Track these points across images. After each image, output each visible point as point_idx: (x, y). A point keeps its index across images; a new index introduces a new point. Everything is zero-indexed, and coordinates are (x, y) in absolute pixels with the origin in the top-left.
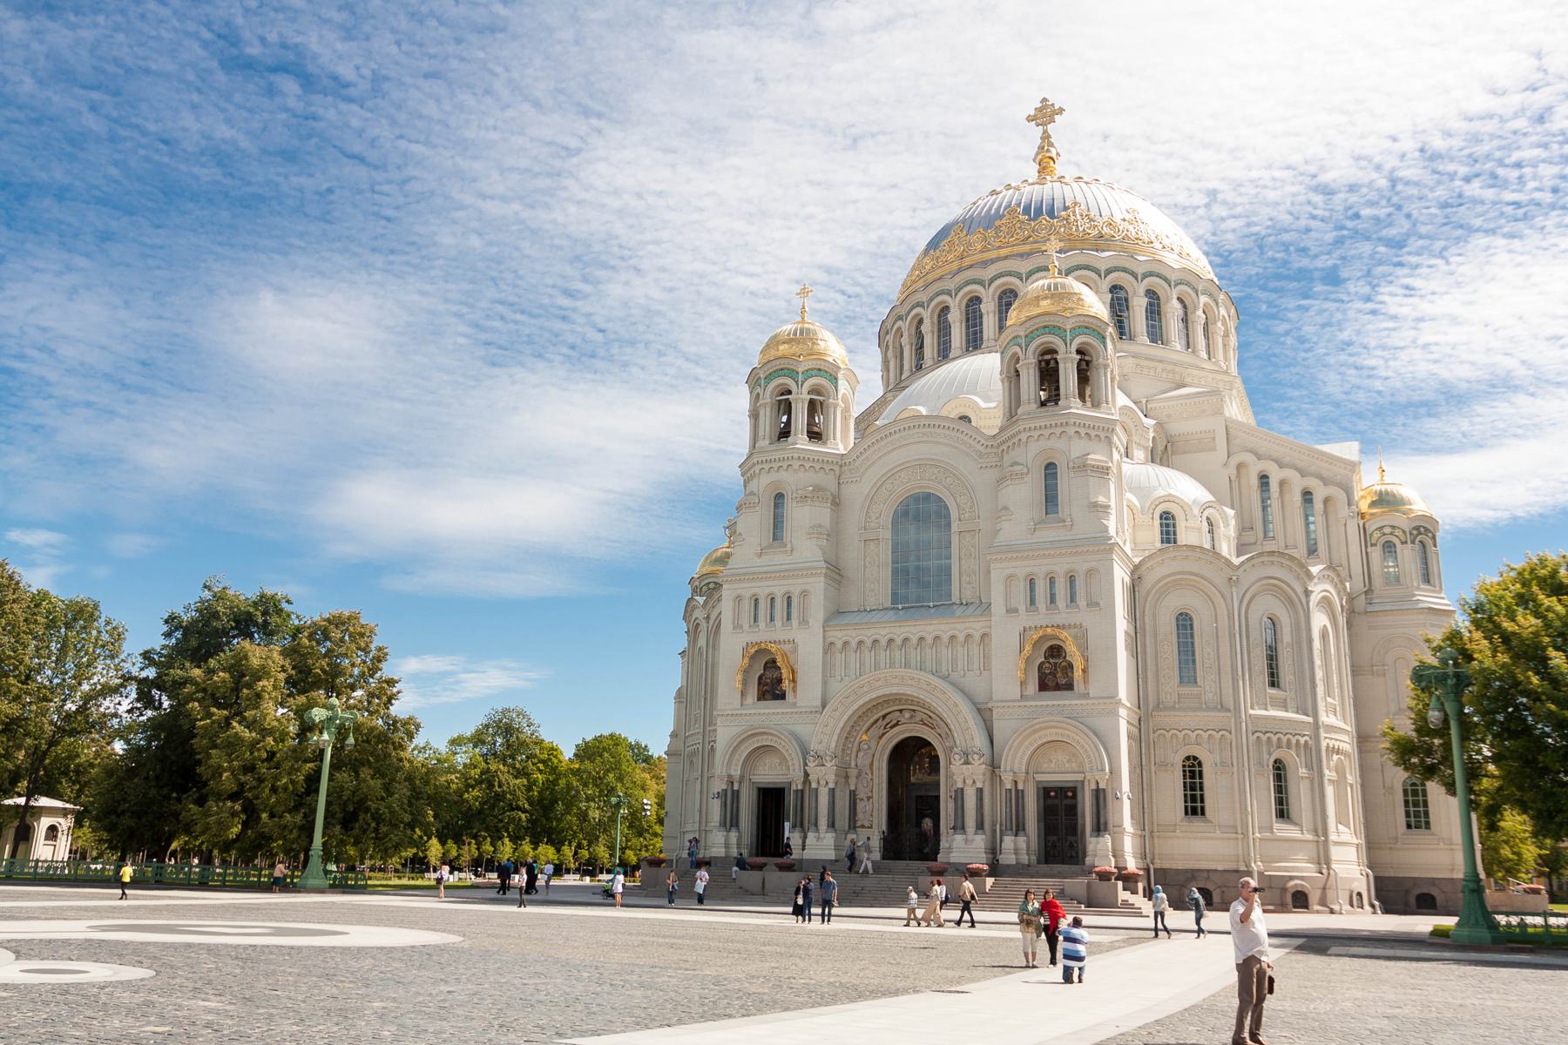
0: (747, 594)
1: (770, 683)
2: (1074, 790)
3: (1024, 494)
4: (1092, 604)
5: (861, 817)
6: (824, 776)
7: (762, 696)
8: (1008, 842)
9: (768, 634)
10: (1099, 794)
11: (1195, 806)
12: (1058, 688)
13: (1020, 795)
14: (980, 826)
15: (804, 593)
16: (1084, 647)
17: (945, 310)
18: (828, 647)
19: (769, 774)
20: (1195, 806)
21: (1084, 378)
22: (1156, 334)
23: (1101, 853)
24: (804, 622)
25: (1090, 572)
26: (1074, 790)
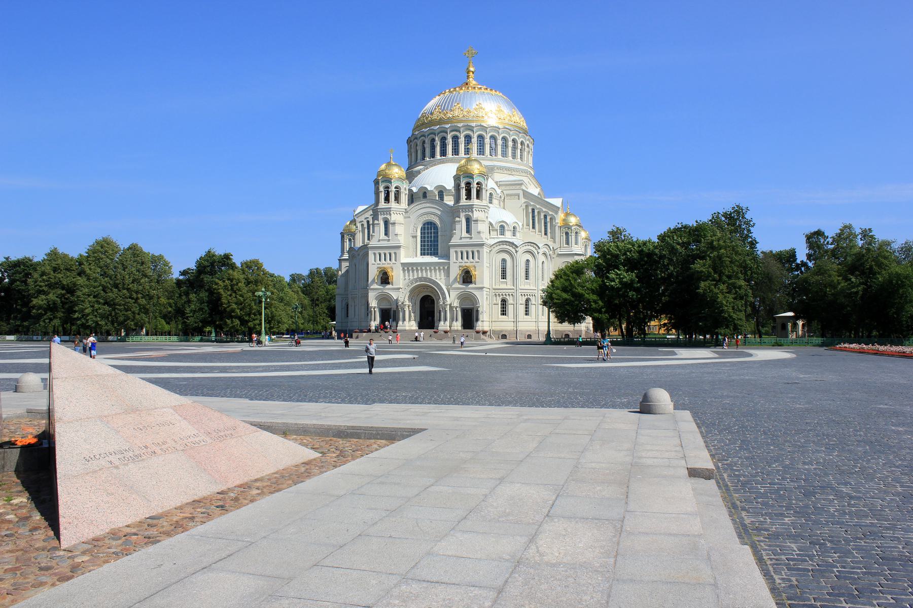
1: (385, 279)
9: (385, 264)
10: (477, 311)
11: (504, 312)
17: (433, 140)
20: (504, 312)
21: (478, 192)
22: (504, 154)
23: (479, 326)
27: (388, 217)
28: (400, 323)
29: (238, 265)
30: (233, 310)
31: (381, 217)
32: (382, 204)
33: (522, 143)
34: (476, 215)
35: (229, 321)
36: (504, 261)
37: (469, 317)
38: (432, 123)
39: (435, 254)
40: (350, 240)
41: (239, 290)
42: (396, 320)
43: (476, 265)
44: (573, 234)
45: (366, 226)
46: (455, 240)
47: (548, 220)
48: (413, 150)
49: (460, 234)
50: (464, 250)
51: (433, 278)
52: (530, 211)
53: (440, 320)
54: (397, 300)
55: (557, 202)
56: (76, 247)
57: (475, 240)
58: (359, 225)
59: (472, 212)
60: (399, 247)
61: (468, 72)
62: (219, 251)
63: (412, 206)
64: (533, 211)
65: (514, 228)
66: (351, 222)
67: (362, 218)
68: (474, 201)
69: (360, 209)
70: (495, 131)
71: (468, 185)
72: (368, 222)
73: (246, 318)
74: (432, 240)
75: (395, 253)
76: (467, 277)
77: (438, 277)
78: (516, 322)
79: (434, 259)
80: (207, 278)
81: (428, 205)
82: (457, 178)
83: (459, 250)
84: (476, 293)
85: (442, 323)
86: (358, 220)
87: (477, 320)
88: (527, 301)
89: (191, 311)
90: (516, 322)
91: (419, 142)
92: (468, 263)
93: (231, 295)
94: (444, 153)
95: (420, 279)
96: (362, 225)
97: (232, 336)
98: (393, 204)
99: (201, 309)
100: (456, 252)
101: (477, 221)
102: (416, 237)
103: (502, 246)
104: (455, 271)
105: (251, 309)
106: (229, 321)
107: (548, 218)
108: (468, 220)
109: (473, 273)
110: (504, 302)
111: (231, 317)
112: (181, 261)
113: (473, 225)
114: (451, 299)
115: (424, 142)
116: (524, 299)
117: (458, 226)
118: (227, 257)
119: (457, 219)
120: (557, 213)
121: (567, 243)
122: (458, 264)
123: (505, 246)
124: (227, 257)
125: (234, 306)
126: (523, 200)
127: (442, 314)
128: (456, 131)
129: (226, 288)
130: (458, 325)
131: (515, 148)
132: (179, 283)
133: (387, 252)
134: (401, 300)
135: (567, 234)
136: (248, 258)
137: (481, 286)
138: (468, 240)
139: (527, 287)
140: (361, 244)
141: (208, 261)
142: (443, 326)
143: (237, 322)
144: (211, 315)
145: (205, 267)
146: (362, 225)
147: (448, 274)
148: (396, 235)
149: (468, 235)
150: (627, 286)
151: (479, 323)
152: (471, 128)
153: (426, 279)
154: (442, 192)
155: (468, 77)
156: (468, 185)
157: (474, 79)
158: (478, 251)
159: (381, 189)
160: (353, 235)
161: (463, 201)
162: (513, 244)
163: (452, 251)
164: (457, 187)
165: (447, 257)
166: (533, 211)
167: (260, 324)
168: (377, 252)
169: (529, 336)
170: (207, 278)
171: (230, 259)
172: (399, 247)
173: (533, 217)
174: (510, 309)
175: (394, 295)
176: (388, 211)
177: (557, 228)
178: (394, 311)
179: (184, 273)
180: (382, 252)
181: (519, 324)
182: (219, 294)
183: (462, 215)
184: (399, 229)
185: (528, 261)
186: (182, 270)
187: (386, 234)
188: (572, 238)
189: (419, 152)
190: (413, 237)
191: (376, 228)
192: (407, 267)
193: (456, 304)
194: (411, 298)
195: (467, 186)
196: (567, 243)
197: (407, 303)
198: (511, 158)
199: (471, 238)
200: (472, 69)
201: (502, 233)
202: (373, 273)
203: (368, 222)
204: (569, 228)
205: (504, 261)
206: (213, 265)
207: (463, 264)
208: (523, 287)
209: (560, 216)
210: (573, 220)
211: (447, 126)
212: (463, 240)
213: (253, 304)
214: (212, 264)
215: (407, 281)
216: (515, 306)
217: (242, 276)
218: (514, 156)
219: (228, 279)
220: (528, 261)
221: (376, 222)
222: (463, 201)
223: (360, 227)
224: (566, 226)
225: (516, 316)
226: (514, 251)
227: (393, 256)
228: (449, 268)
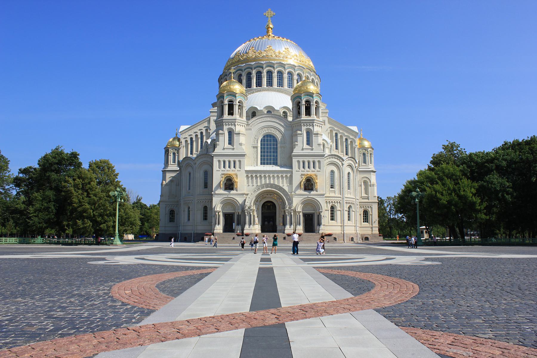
1: (229, 184)
2: (312, 215)
9: (230, 171)
10: (319, 216)
12: (309, 190)
17: (249, 74)
26: (312, 215)
27: (233, 127)
28: (247, 226)
29: (85, 166)
30: (85, 211)
31: (226, 128)
32: (226, 116)
34: (316, 129)
35: (79, 222)
36: (332, 172)
37: (311, 222)
38: (247, 60)
39: (276, 164)
40: (174, 154)
41: (91, 189)
42: (241, 223)
43: (318, 173)
44: (369, 155)
45: (189, 142)
46: (297, 151)
47: (349, 143)
49: (301, 146)
50: (306, 159)
51: (281, 185)
52: (334, 135)
53: (284, 224)
54: (243, 206)
55: (355, 129)
57: (317, 150)
58: (183, 141)
59: (313, 126)
60: (244, 155)
61: (268, 28)
62: (67, 150)
63: (254, 119)
64: (336, 134)
65: (331, 146)
66: (174, 139)
67: (186, 135)
68: (313, 117)
69: (183, 128)
70: (302, 70)
71: (308, 102)
72: (191, 139)
73: (99, 219)
74: (272, 150)
75: (240, 161)
76: (309, 185)
77: (283, 183)
78: (343, 226)
79: (277, 168)
80: (54, 176)
81: (269, 119)
82: (293, 99)
83: (301, 159)
84: (319, 199)
85: (288, 227)
86: (182, 137)
87: (319, 224)
88: (350, 207)
89: (35, 211)
90: (343, 226)
92: (310, 172)
93: (82, 194)
94: (259, 84)
95: (267, 185)
96: (186, 141)
97: (78, 236)
98: (236, 116)
99: (47, 209)
100: (299, 162)
101: (317, 134)
102: (257, 147)
103: (331, 159)
104: (298, 178)
105: (105, 210)
106: (79, 222)
107: (349, 141)
108: (309, 134)
110: (332, 208)
111: (82, 217)
112: (24, 158)
113: (314, 138)
114: (297, 203)
116: (348, 207)
117: (299, 139)
118: (74, 155)
119: (299, 132)
120: (356, 137)
121: (365, 162)
122: (301, 173)
123: (334, 160)
124: (74, 155)
125: (88, 206)
126: (328, 126)
127: (288, 218)
128: (271, 66)
129: (76, 186)
130: (300, 229)
133: (232, 160)
134: (247, 204)
135: (364, 154)
136: (97, 158)
137: (321, 192)
138: (310, 151)
139: (349, 196)
140: (184, 157)
141: (55, 158)
142: (289, 229)
143: (89, 223)
144: (57, 214)
145: (51, 164)
146: (186, 141)
147: (290, 180)
148: (241, 144)
149: (308, 147)
150: (504, 190)
151: (322, 227)
152: (282, 65)
153: (272, 186)
154: (270, 111)
155: (268, 32)
156: (308, 102)
157: (272, 34)
158: (319, 162)
159: (226, 102)
160: (178, 149)
161: (304, 117)
162: (340, 158)
163: (295, 161)
164: (297, 105)
165: (291, 167)
166: (336, 134)
167: (114, 227)
168: (222, 159)
169: (352, 239)
170: (54, 176)
172: (244, 155)
173: (336, 140)
174: (338, 214)
175: (240, 200)
176: (233, 122)
177: (356, 150)
178: (239, 216)
179: (25, 171)
180: (227, 160)
181: (346, 228)
182: (69, 192)
183: (304, 128)
184: (242, 139)
185: (349, 173)
186: (23, 168)
187: (230, 143)
188: (368, 158)
190: (254, 147)
191: (221, 138)
192: (251, 174)
193: (299, 209)
194: (256, 201)
195: (303, 106)
196: (365, 162)
197: (254, 208)
199: (312, 149)
200: (271, 26)
202: (218, 178)
203: (191, 139)
204: (366, 149)
205: (332, 172)
206: (58, 164)
207: (305, 173)
208: (346, 196)
209: (357, 142)
210: (366, 144)
211: (262, 62)
212: (305, 151)
213: (108, 205)
214: (60, 163)
215: (255, 186)
216: (342, 211)
217: (94, 176)
219: (79, 178)
220: (349, 173)
221: (221, 132)
222: (304, 117)
223: (184, 143)
224: (363, 147)
225: (343, 221)
226: (340, 163)
227: (237, 164)
228: (291, 176)
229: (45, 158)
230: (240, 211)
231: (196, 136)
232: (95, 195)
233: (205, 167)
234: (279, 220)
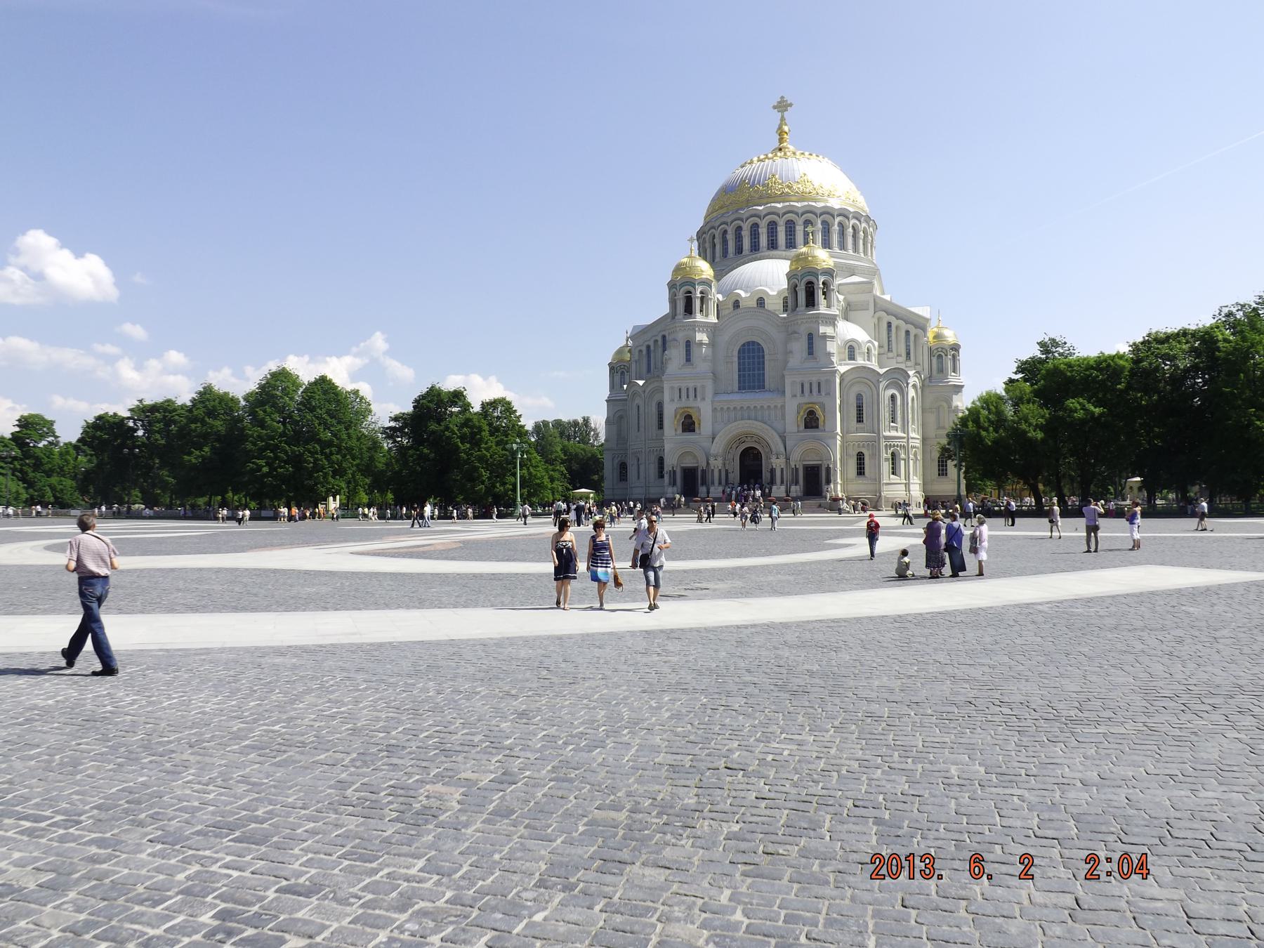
0: (676, 386)
1: (689, 425)
3: (799, 346)
4: (828, 394)
5: (731, 480)
6: (716, 464)
7: (684, 431)
8: (793, 488)
10: (828, 469)
13: (797, 470)
14: (782, 482)
15: (703, 387)
16: (824, 411)
18: (714, 410)
19: (689, 463)
22: (843, 246)
24: (703, 399)
25: (827, 381)
33: (865, 232)
47: (912, 338)
48: (707, 245)
56: (239, 383)
91: (718, 233)
109: (819, 413)
115: (725, 232)
131: (855, 236)
132: (390, 433)
139: (893, 433)
167: (514, 490)
171: (465, 397)
179: (395, 419)
185: (893, 397)
189: (718, 247)
198: (851, 252)
201: (852, 357)
203: (648, 347)
208: (887, 434)
218: (856, 249)
220: (893, 397)
229: (423, 397)
230: (704, 465)
231: (656, 341)
232: (487, 449)
233: (657, 398)
234: (766, 475)
